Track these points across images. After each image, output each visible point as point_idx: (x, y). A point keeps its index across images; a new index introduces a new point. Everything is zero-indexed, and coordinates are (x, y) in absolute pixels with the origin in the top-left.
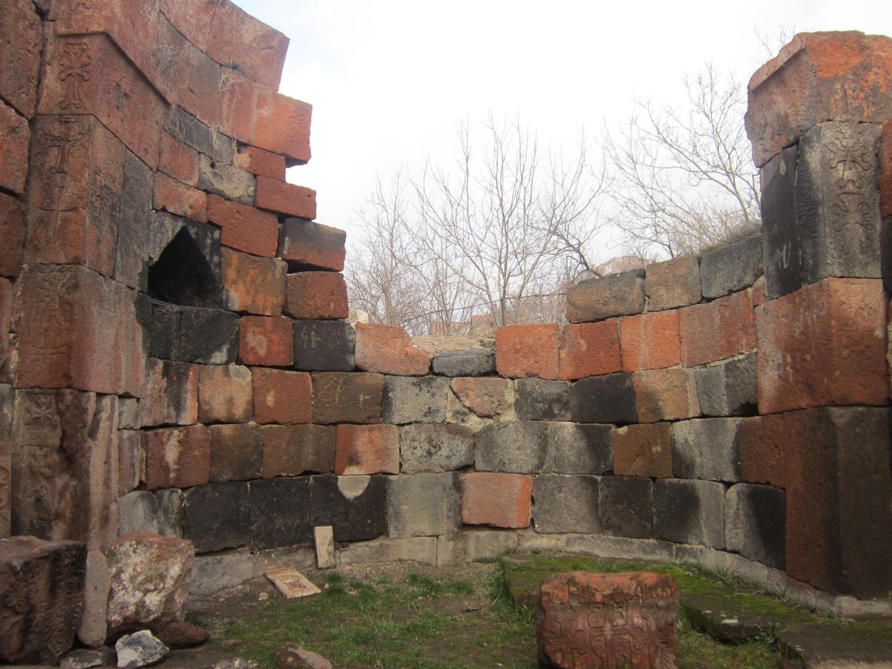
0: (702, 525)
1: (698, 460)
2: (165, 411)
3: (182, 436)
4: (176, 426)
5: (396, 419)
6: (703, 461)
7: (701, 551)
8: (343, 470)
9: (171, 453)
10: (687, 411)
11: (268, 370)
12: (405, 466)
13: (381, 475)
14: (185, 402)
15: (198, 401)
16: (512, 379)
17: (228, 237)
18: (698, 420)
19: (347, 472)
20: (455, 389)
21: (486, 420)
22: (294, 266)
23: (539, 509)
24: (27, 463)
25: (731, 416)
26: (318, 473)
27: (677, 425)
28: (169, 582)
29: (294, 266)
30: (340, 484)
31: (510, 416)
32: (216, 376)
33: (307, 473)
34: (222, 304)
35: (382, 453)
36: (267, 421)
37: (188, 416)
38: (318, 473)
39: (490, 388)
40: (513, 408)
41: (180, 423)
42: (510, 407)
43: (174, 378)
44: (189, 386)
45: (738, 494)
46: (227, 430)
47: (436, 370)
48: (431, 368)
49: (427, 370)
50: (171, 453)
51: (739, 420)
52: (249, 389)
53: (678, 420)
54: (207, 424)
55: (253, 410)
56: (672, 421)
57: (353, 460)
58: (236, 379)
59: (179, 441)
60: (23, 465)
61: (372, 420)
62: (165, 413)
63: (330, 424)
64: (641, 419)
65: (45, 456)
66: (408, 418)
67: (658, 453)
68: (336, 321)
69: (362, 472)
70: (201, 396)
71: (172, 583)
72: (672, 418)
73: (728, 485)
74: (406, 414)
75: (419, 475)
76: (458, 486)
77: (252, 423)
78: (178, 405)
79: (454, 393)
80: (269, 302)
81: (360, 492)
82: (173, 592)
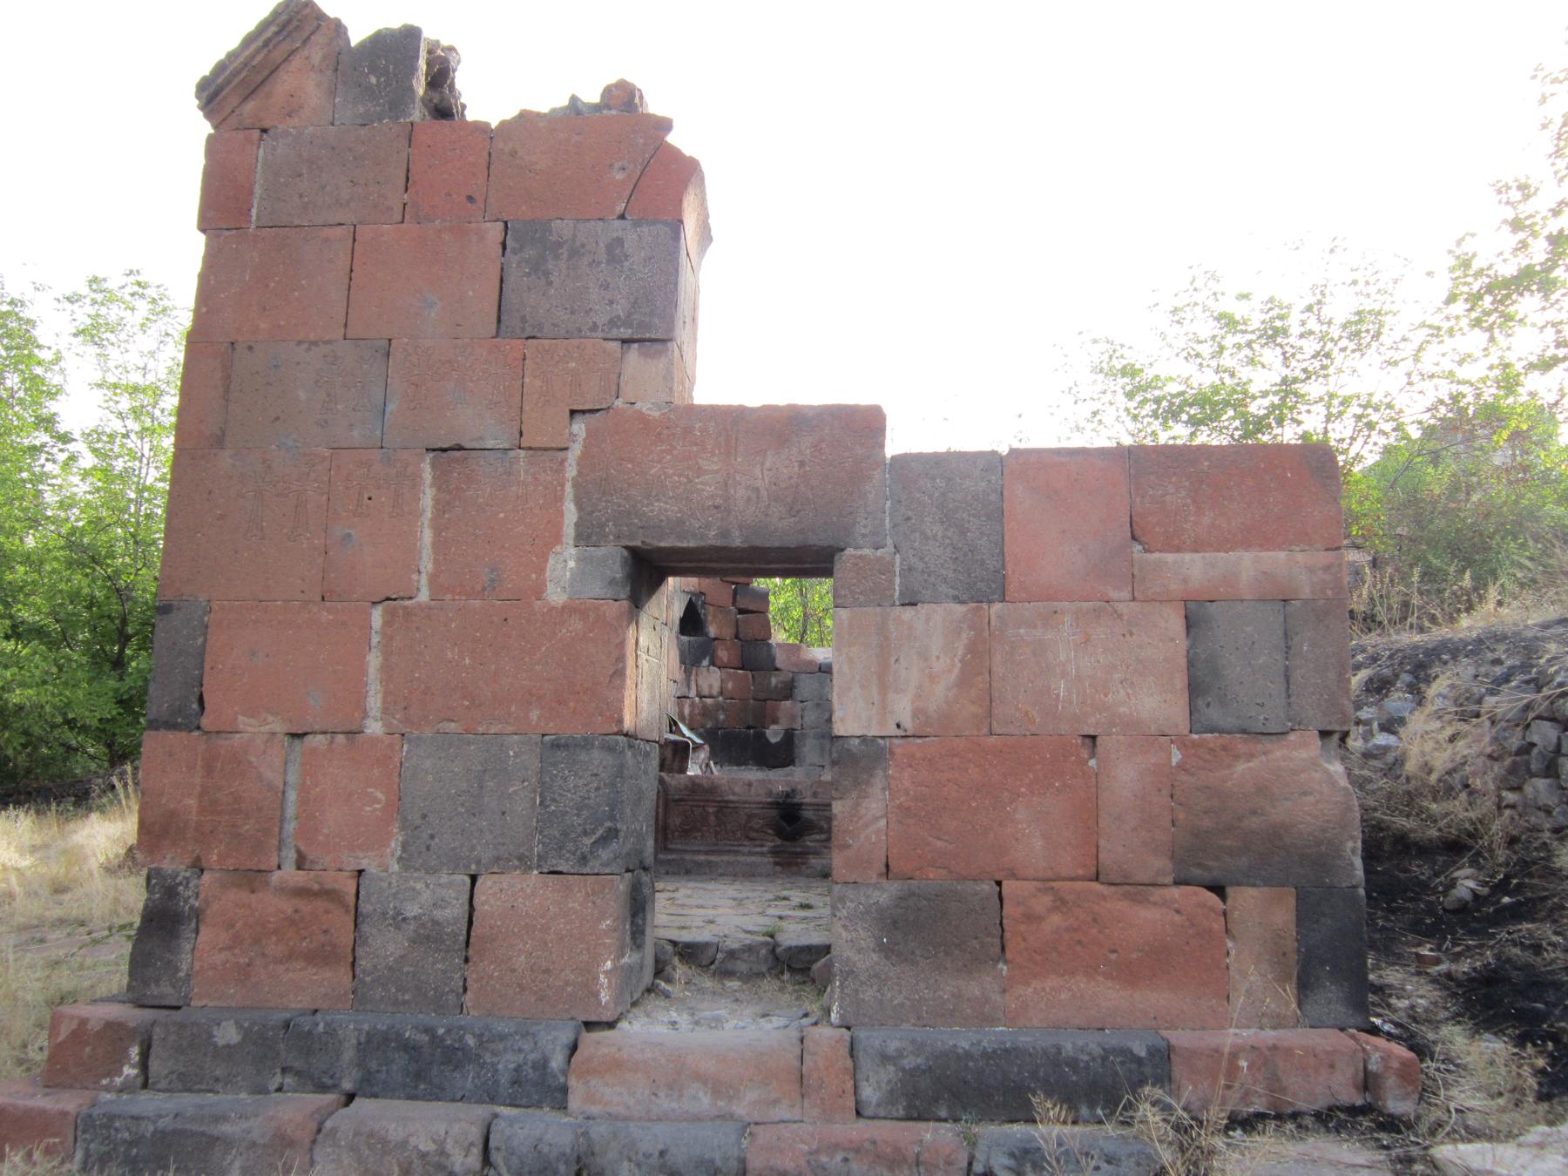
9: (687, 711)
17: (709, 599)
22: (741, 611)
29: (741, 611)
34: (706, 635)
35: (793, 718)
37: (693, 693)
43: (687, 672)
46: (709, 701)
50: (687, 711)
55: (721, 693)
57: (775, 721)
62: (684, 691)
68: (763, 639)
78: (689, 686)
80: (728, 633)
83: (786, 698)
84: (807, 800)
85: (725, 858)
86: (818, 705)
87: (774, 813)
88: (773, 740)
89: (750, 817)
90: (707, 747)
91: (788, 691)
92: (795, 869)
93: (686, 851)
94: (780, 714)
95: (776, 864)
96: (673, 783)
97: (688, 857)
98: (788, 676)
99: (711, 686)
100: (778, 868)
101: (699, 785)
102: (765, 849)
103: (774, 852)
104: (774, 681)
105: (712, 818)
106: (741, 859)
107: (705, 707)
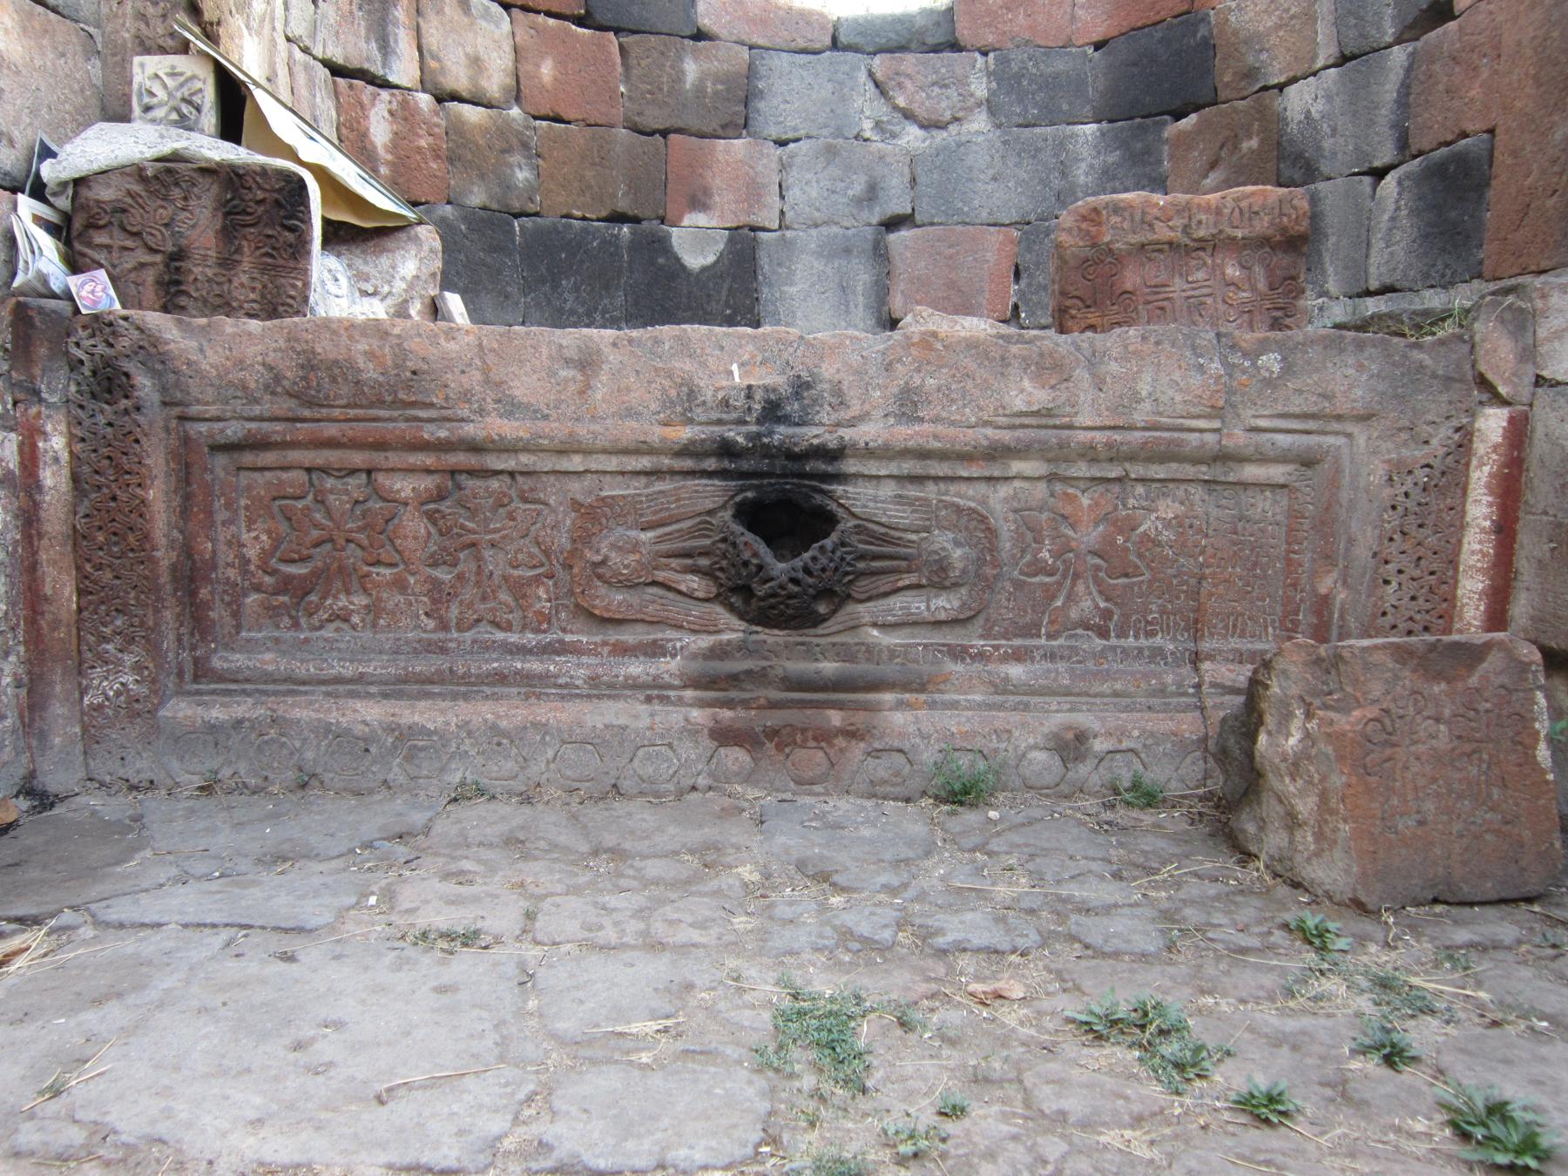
0: (1327, 258)
1: (1327, 144)
2: (363, 44)
3: (394, 106)
4: (385, 84)
5: (774, 132)
6: (1337, 149)
7: (1321, 309)
8: (681, 218)
9: (380, 131)
10: (1314, 58)
11: (541, 18)
12: (789, 215)
13: (746, 231)
14: (396, 41)
15: (420, 49)
16: (985, 54)
18: (1332, 70)
19: (686, 221)
20: (879, 75)
21: (935, 132)
23: (1030, 285)
24: (133, 31)
25: (1399, 41)
26: (636, 220)
27: (1292, 90)
28: (399, 286)
30: (675, 241)
31: (979, 123)
32: (447, 9)
33: (618, 218)
36: (543, 112)
38: (636, 220)
39: (943, 70)
40: (984, 107)
41: (392, 79)
42: (979, 105)
44: (400, 13)
45: (1399, 183)
47: (843, 39)
48: (834, 39)
49: (828, 41)
51: (1410, 47)
52: (507, 47)
53: (1293, 80)
54: (440, 100)
55: (517, 94)
56: (1281, 87)
57: (698, 202)
58: (484, 24)
59: (391, 113)
60: (127, 35)
61: (730, 132)
63: (651, 134)
64: (1223, 95)
65: (164, 16)
66: (795, 129)
67: (1252, 151)
69: (714, 223)
70: (424, 41)
71: (404, 286)
72: (1282, 79)
73: (1379, 174)
74: (790, 123)
75: (814, 232)
76: (880, 253)
77: (515, 112)
78: (385, 47)
79: (877, 85)
81: (711, 259)
82: (406, 301)
83: (741, 125)
84: (870, 432)
85: (481, 712)
86: (831, 152)
87: (709, 495)
88: (696, 258)
89: (592, 515)
90: (428, 235)
91: (737, 107)
92: (815, 758)
93: (293, 684)
94: (717, 182)
95: (724, 736)
96: (211, 360)
97: (301, 711)
98: (735, 58)
99: (476, 62)
100: (736, 757)
101: (340, 370)
102: (669, 667)
103: (712, 682)
104: (691, 69)
105: (414, 526)
106: (550, 712)
107: (456, 129)
